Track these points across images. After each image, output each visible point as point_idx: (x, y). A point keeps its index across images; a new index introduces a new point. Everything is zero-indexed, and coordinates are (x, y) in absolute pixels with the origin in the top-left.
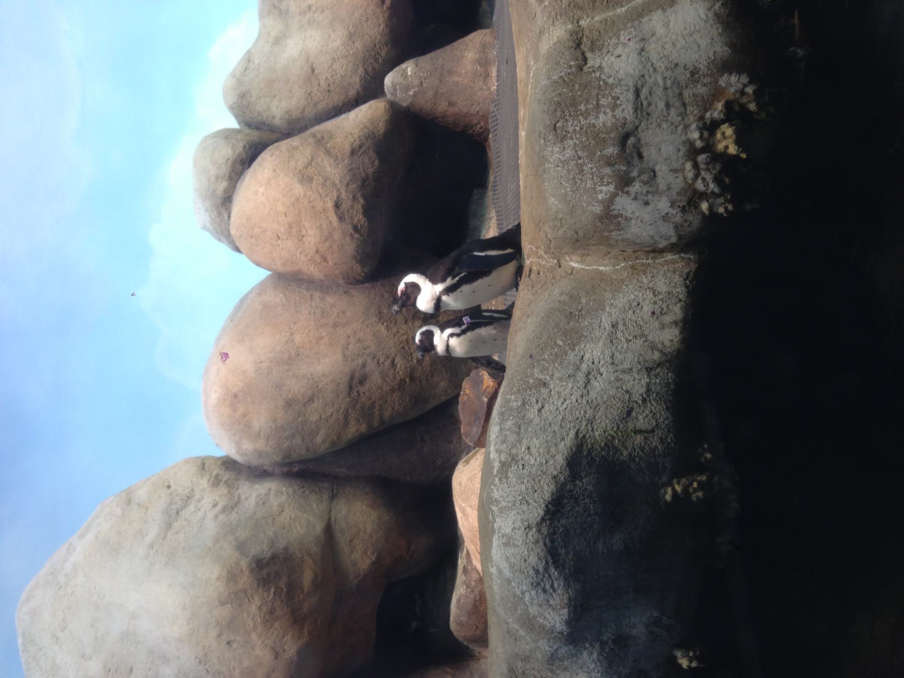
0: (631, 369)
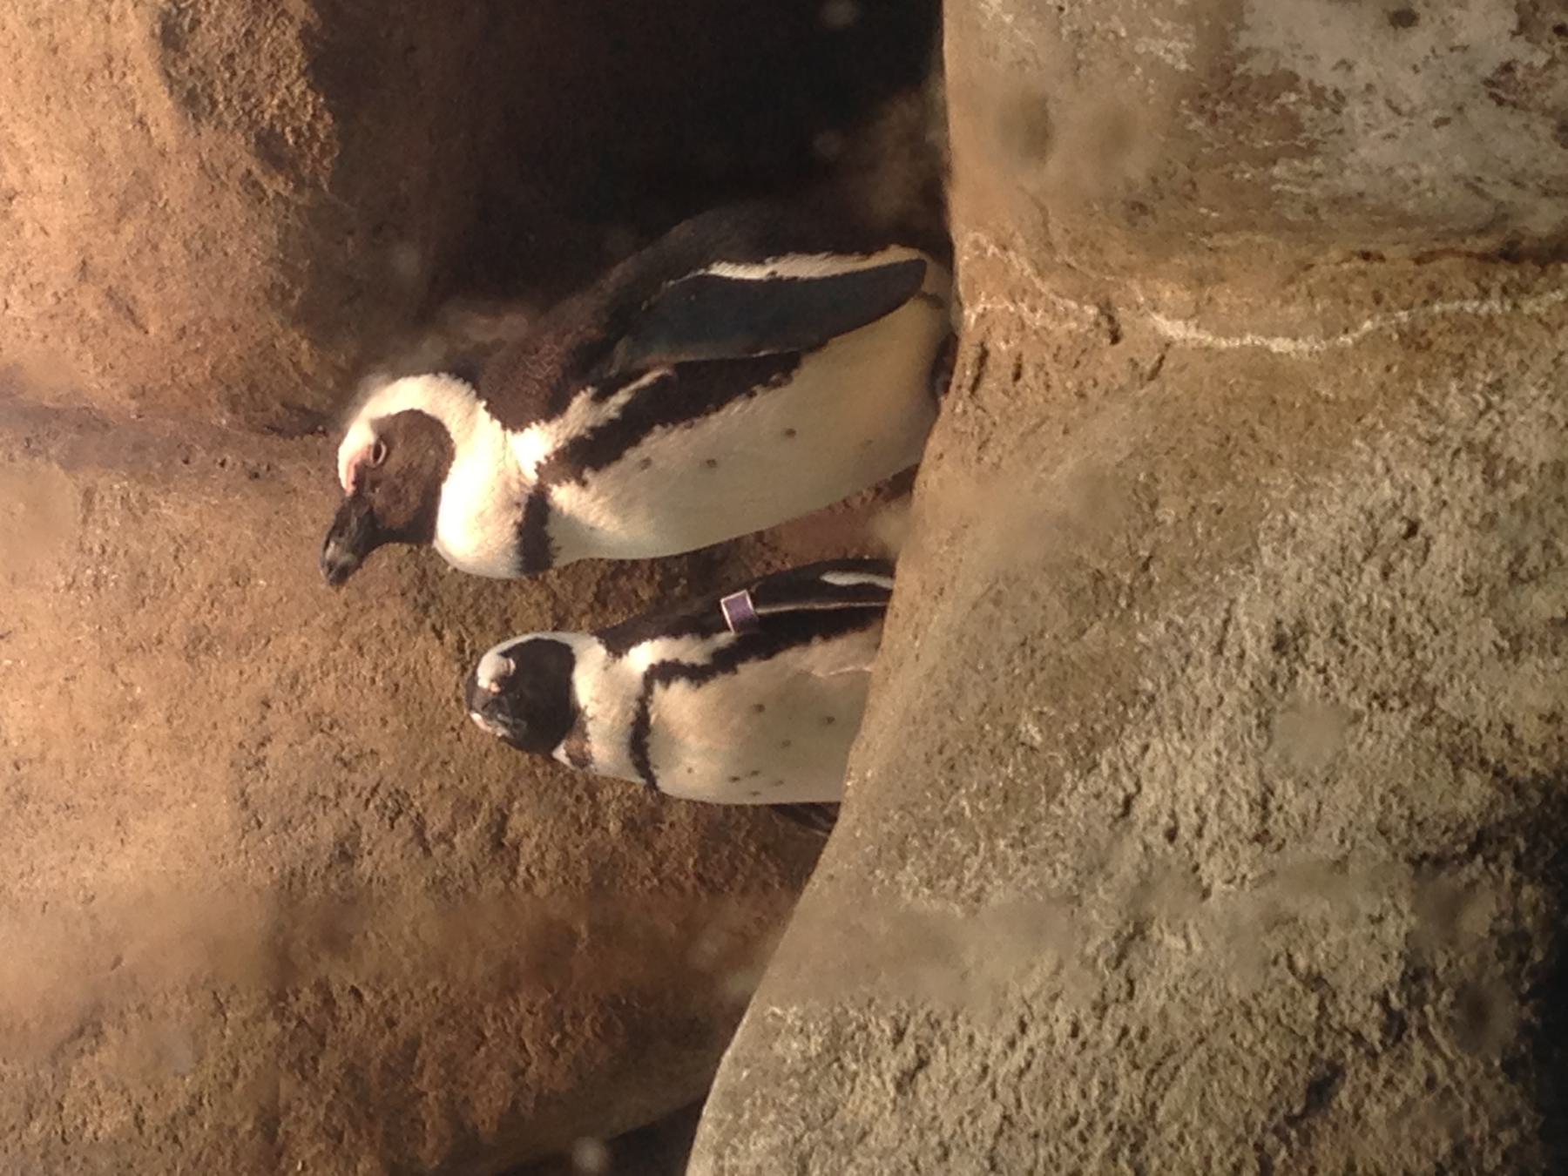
0: (1341, 864)
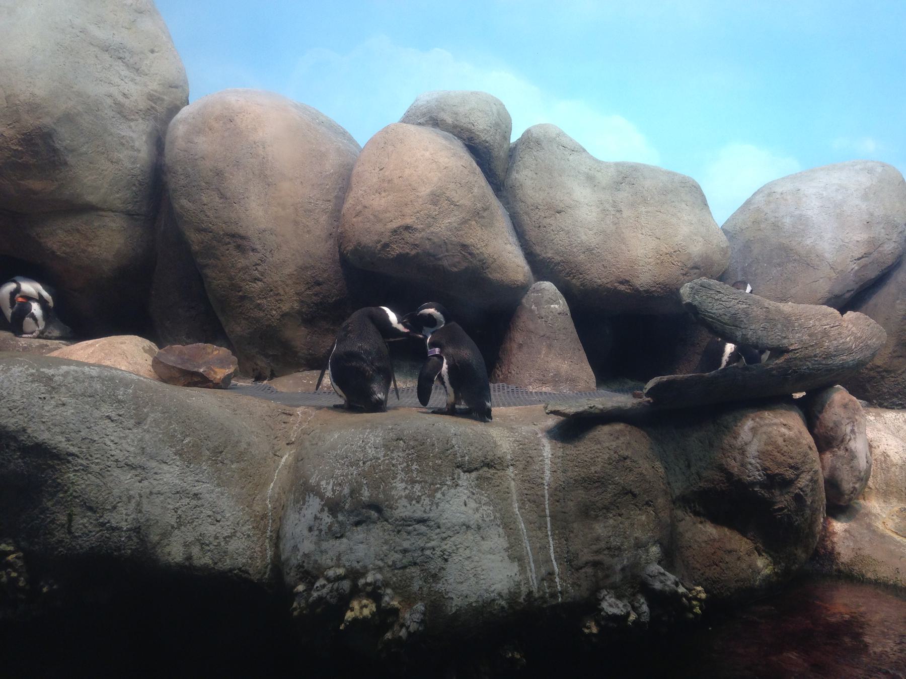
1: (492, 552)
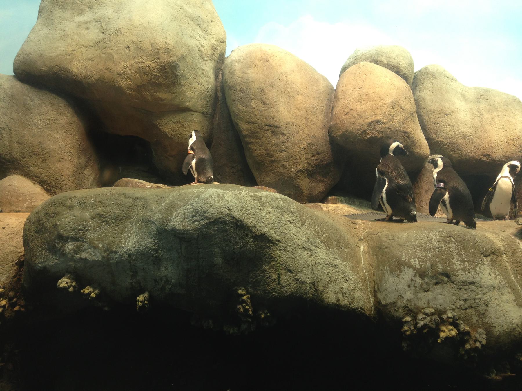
0: (314, 273)
1: (508, 302)
